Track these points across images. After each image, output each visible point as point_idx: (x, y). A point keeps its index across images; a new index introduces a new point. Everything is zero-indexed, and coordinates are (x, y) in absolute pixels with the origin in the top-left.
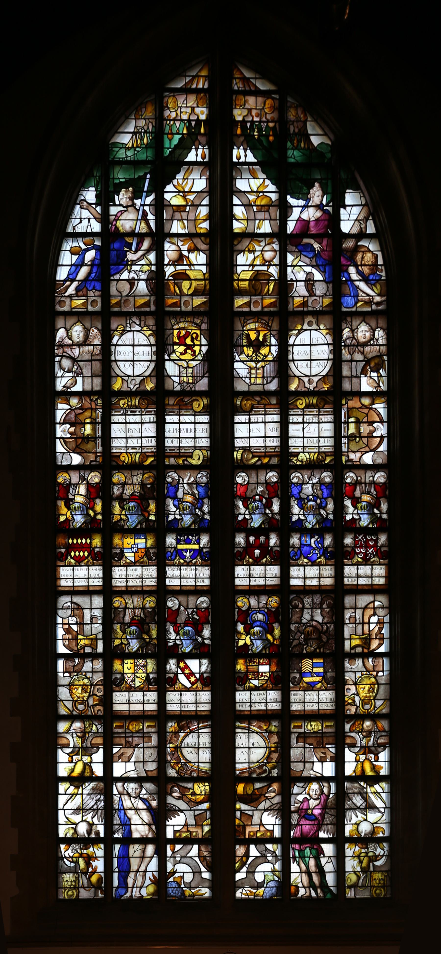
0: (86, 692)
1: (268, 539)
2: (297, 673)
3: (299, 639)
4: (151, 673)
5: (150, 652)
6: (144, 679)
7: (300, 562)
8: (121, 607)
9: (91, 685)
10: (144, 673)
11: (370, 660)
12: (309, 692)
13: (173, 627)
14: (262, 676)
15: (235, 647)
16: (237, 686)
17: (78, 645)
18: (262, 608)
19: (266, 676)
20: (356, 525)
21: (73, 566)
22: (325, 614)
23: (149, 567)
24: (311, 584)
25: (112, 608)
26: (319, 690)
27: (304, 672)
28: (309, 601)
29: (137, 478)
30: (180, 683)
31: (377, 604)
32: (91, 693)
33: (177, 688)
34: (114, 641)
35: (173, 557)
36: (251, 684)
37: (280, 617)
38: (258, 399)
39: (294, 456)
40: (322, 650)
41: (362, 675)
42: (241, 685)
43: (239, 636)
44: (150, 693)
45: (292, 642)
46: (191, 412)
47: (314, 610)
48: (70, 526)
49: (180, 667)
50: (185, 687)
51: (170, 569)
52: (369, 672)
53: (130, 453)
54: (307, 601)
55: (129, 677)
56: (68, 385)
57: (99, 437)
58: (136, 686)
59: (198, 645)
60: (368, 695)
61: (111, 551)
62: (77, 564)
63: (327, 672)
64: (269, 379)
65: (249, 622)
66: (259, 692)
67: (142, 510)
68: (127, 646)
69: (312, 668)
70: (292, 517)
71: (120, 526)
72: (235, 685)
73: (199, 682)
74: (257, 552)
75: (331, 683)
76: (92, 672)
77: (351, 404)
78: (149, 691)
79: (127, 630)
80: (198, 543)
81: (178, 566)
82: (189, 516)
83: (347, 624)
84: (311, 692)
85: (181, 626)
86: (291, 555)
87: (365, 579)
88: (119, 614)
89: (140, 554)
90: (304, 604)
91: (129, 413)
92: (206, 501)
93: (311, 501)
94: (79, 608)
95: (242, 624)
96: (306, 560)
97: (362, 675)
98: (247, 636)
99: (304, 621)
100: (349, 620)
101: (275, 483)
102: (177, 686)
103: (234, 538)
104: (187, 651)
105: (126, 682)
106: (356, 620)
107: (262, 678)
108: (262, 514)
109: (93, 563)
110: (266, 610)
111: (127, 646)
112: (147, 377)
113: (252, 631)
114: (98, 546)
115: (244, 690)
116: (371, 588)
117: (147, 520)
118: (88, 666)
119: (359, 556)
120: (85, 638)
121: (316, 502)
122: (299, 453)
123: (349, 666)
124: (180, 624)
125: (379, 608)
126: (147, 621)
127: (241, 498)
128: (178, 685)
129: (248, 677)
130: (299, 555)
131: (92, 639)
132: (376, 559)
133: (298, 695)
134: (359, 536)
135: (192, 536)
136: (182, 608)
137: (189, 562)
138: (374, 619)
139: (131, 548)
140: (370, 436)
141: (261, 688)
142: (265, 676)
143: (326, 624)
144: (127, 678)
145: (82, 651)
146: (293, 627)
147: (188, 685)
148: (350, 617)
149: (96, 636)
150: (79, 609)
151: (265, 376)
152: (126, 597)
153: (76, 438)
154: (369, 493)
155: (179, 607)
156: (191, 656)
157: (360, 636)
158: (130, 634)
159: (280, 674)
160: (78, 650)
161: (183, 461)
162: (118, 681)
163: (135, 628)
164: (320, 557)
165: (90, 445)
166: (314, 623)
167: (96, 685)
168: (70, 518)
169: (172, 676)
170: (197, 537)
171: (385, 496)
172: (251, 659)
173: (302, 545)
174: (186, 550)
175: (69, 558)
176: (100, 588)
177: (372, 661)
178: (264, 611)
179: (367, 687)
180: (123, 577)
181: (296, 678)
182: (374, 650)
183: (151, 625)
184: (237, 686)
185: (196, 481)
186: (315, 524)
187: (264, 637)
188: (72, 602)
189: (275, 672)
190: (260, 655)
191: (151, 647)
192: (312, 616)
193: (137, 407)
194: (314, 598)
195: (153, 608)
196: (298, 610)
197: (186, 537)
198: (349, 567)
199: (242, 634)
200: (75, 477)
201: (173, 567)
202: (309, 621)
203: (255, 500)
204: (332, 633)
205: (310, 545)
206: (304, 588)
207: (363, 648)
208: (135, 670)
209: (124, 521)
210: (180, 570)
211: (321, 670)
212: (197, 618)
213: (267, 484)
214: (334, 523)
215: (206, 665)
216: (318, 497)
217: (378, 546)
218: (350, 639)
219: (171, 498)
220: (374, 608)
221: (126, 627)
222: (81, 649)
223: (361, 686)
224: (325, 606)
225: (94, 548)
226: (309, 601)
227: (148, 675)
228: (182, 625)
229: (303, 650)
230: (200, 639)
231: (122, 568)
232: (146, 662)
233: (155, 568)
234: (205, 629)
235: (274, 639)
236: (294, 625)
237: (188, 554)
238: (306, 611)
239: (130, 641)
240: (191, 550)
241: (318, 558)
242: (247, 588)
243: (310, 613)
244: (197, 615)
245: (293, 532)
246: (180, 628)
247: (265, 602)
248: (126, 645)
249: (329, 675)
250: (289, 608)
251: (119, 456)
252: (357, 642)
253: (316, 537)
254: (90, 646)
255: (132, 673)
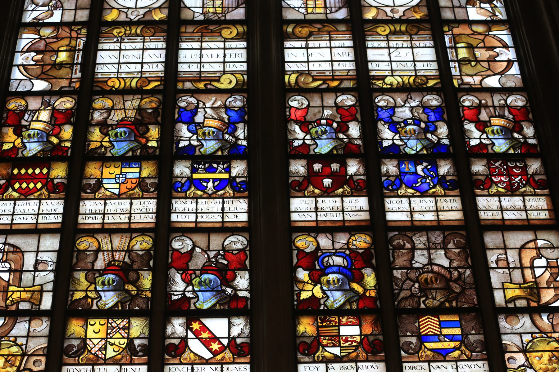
0: (12, 366)
1: (344, 166)
2: (412, 336)
3: (410, 289)
4: (138, 338)
5: (137, 308)
6: (124, 346)
7: (401, 192)
8: (90, 249)
9: (23, 355)
10: (124, 338)
11: (545, 317)
12: (439, 364)
13: (181, 274)
14: (346, 341)
15: (294, 300)
16: (300, 355)
17: (7, 299)
18: (340, 249)
19: (355, 342)
20: (488, 150)
21: (15, 200)
22: (453, 257)
23: (143, 200)
24: (424, 219)
25: (73, 251)
26: (456, 361)
27: (426, 335)
28: (421, 239)
29: (132, 103)
30: (192, 352)
31: (540, 243)
32: (22, 367)
33: (186, 359)
34: (73, 294)
35: (184, 188)
36: (326, 354)
37: (374, 261)
38: (319, 26)
39: (379, 80)
40: (454, 304)
41: (534, 338)
42: (307, 355)
43: (300, 286)
44: (134, 367)
45: (399, 294)
46: (219, 38)
47: (432, 251)
48: (18, 154)
49: (191, 330)
50: (201, 358)
51: (179, 202)
52: (545, 333)
53: (123, 78)
54: (420, 240)
55: (95, 345)
56: (40, 17)
57: (77, 63)
58: (107, 358)
59: (226, 298)
60: (550, 367)
61: (81, 182)
62: (23, 197)
63: (467, 335)
64: (333, 9)
65: (318, 267)
66: (342, 365)
67: (135, 136)
68: (95, 301)
69: (440, 328)
70: (381, 143)
71: (100, 154)
72: (296, 355)
73: (227, 351)
74: (327, 182)
75: (478, 349)
76: (28, 337)
77: (456, 31)
78: (131, 363)
79: (97, 280)
80: (228, 170)
81: (193, 198)
82: (213, 142)
83: (494, 268)
84: (444, 364)
85: (195, 273)
86: (385, 185)
87: (515, 212)
88: (86, 258)
89: (129, 185)
90: (414, 244)
91: (126, 40)
92: (240, 126)
93: (410, 124)
94: (17, 250)
95: (305, 270)
96: (410, 191)
97: (534, 338)
98: (315, 286)
99: (416, 265)
100: (497, 264)
101: (351, 106)
102: (184, 356)
103: (288, 165)
104: (205, 307)
105: (89, 351)
106: (508, 263)
107: (347, 344)
108: (332, 138)
109: (49, 195)
110: (347, 252)
111: (95, 301)
112: (155, 8)
113: (324, 279)
114: (60, 177)
115: (314, 362)
116: (526, 223)
117: (145, 147)
118: (21, 328)
119: (499, 185)
120: (22, 289)
121: (419, 125)
122: (386, 76)
123: (507, 326)
124: (194, 270)
125: (547, 248)
126: (135, 267)
127: (297, 122)
128: (187, 355)
129: (319, 343)
130: (398, 185)
131: (34, 291)
132: (528, 189)
133: (418, 368)
134: (495, 163)
135: (218, 164)
136: (198, 250)
137: (212, 194)
138: (541, 262)
139: (115, 179)
140: (492, 60)
141: (345, 359)
142: (352, 341)
143: (456, 268)
144: (92, 346)
145: (14, 308)
146: (397, 274)
147: (207, 355)
148: (497, 261)
149: (42, 288)
150: (16, 252)
151: (328, 5)
152: (100, 237)
153: (43, 65)
154: (502, 116)
155: (193, 249)
156: (212, 313)
157: (520, 284)
158: (103, 283)
159: (381, 338)
160: (7, 306)
161: (205, 85)
162: (75, 350)
163: (112, 276)
164: (434, 187)
165: (64, 72)
166: (435, 268)
167: (32, 355)
168: (20, 145)
169: (176, 342)
170: (225, 166)
171: (528, 120)
172: (325, 318)
173: (402, 174)
174: (207, 181)
175: (10, 190)
176: (59, 226)
177: (548, 319)
178: (344, 253)
179: (546, 356)
180: (98, 212)
181: (411, 343)
182: (548, 303)
183: (141, 272)
184: (300, 355)
185: (225, 105)
186: (421, 150)
187: (347, 287)
188: (5, 244)
189: (370, 335)
190: (340, 312)
191: (139, 301)
192: (430, 259)
193: (138, 35)
194: (430, 236)
195: (148, 251)
196: (404, 251)
197: (207, 165)
198: (484, 198)
199: (307, 283)
200: (34, 103)
201: (184, 200)
202: (425, 265)
203: (320, 124)
204: (470, 280)
205: (415, 173)
206: (412, 223)
207: (528, 300)
208: (107, 334)
209: (106, 148)
210: (197, 203)
211: (458, 331)
212: (226, 262)
213: (338, 107)
214: (451, 148)
215: (242, 326)
216: (420, 121)
217: (528, 175)
218: (504, 289)
219: (184, 123)
220: (537, 248)
221: (97, 275)
222: (12, 305)
223: (534, 354)
224: (451, 246)
225: (52, 180)
226: (421, 239)
227: (131, 341)
228: (198, 272)
229: (420, 304)
230: (229, 290)
231: (98, 202)
232: (129, 322)
233: (155, 201)
234: (238, 277)
235: (366, 290)
236: (400, 271)
237: (210, 185)
238: (417, 253)
239: (102, 293)
240: (215, 180)
241: (431, 189)
242: (314, 224)
243: (427, 255)
244: (225, 259)
245: (386, 158)
246: (193, 276)
247: (345, 242)
248: (93, 299)
249: (472, 338)
250: (389, 249)
251: (106, 82)
252: (517, 292)
253: (425, 164)
254: (28, 301)
255: (102, 339)
